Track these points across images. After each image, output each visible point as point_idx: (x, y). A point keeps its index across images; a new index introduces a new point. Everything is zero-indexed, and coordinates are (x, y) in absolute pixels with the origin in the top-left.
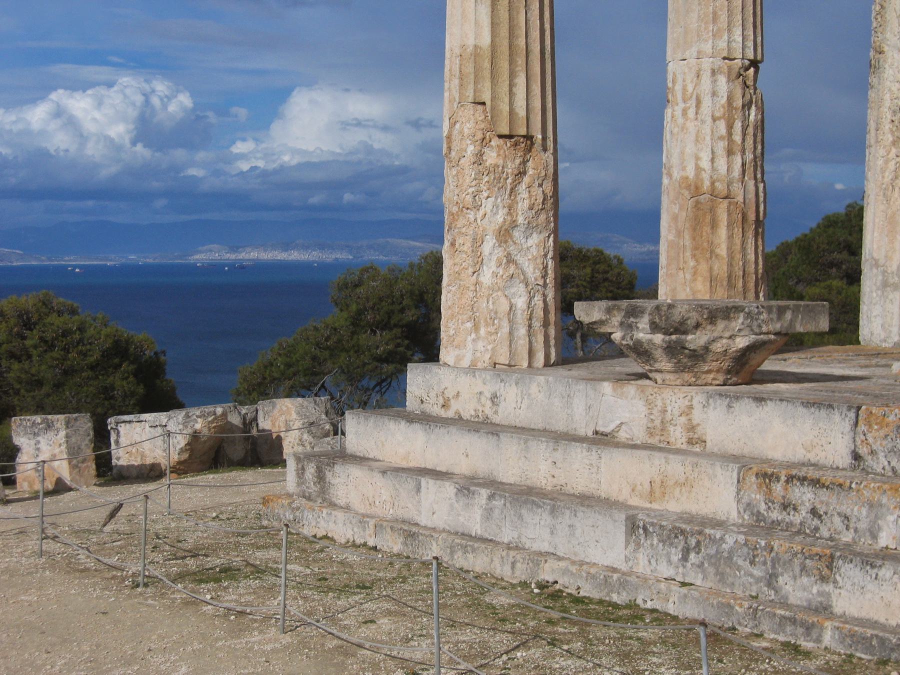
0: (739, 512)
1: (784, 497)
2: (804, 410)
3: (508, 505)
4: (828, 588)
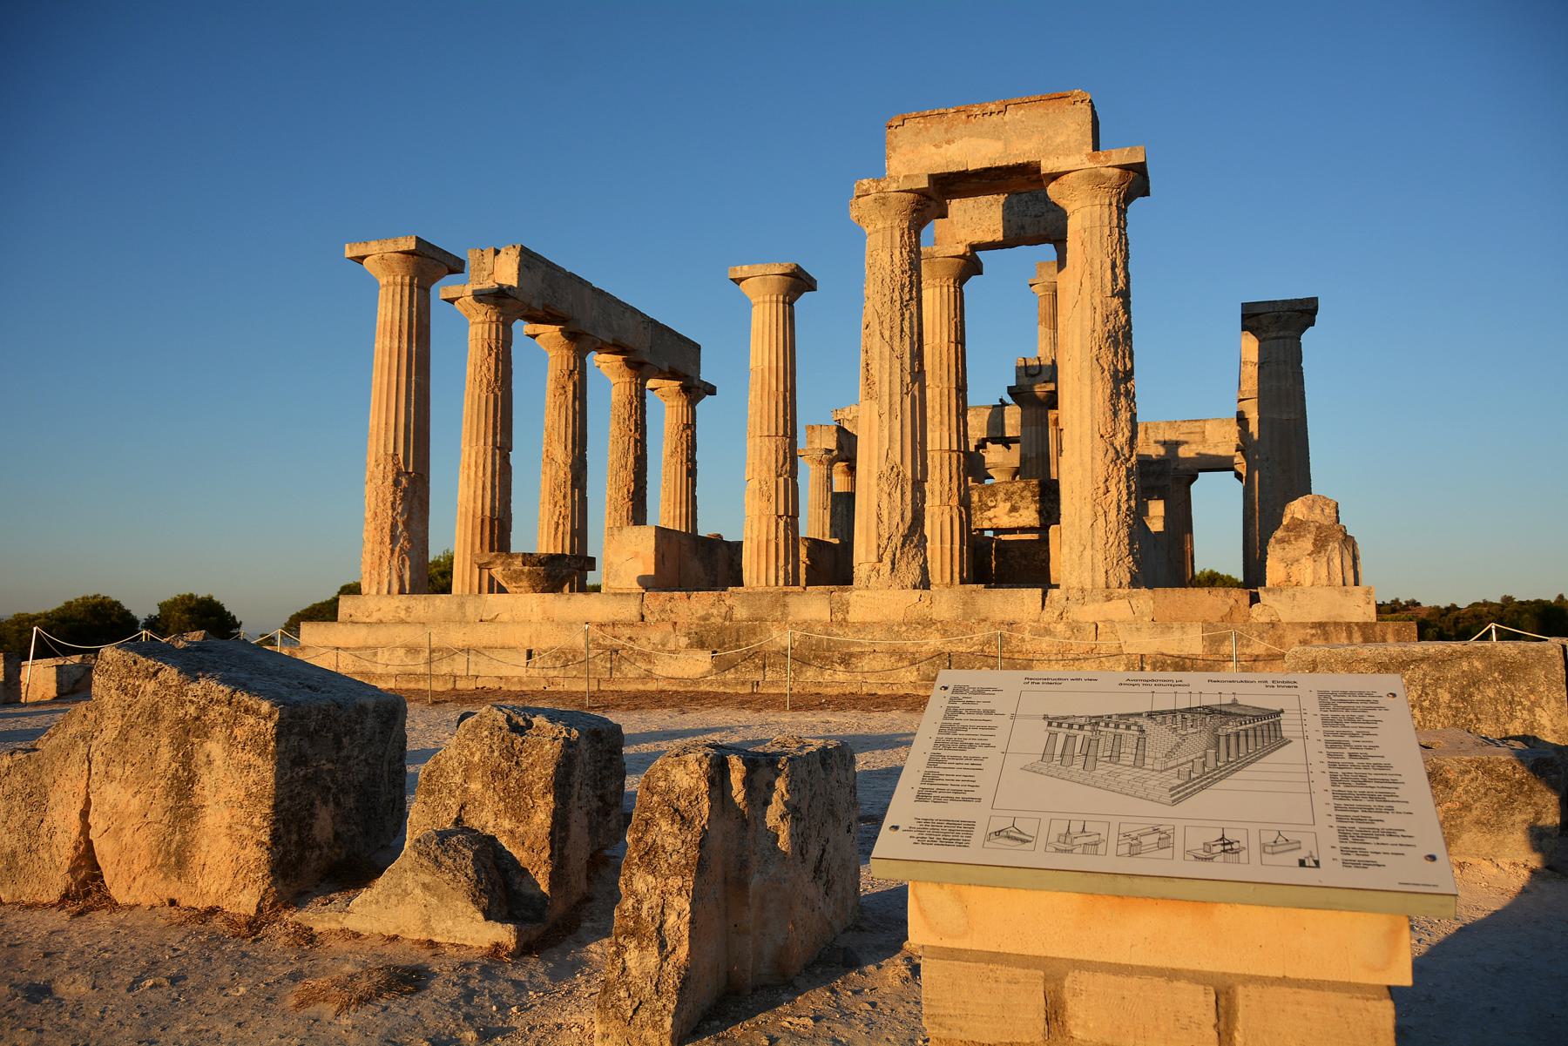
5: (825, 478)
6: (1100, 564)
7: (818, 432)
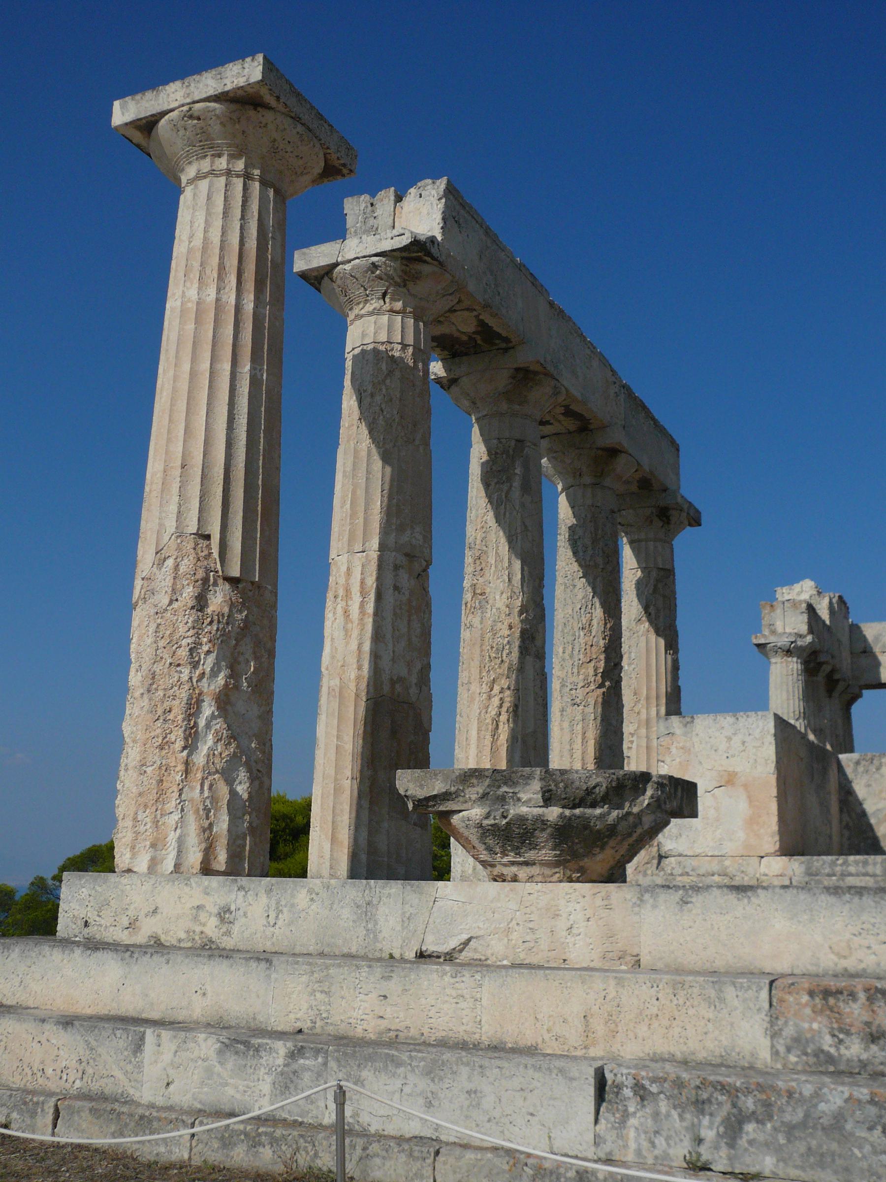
0: (775, 1053)
1: (868, 1024)
2: (832, 899)
3: (332, 1064)
5: (795, 675)
7: (779, 611)
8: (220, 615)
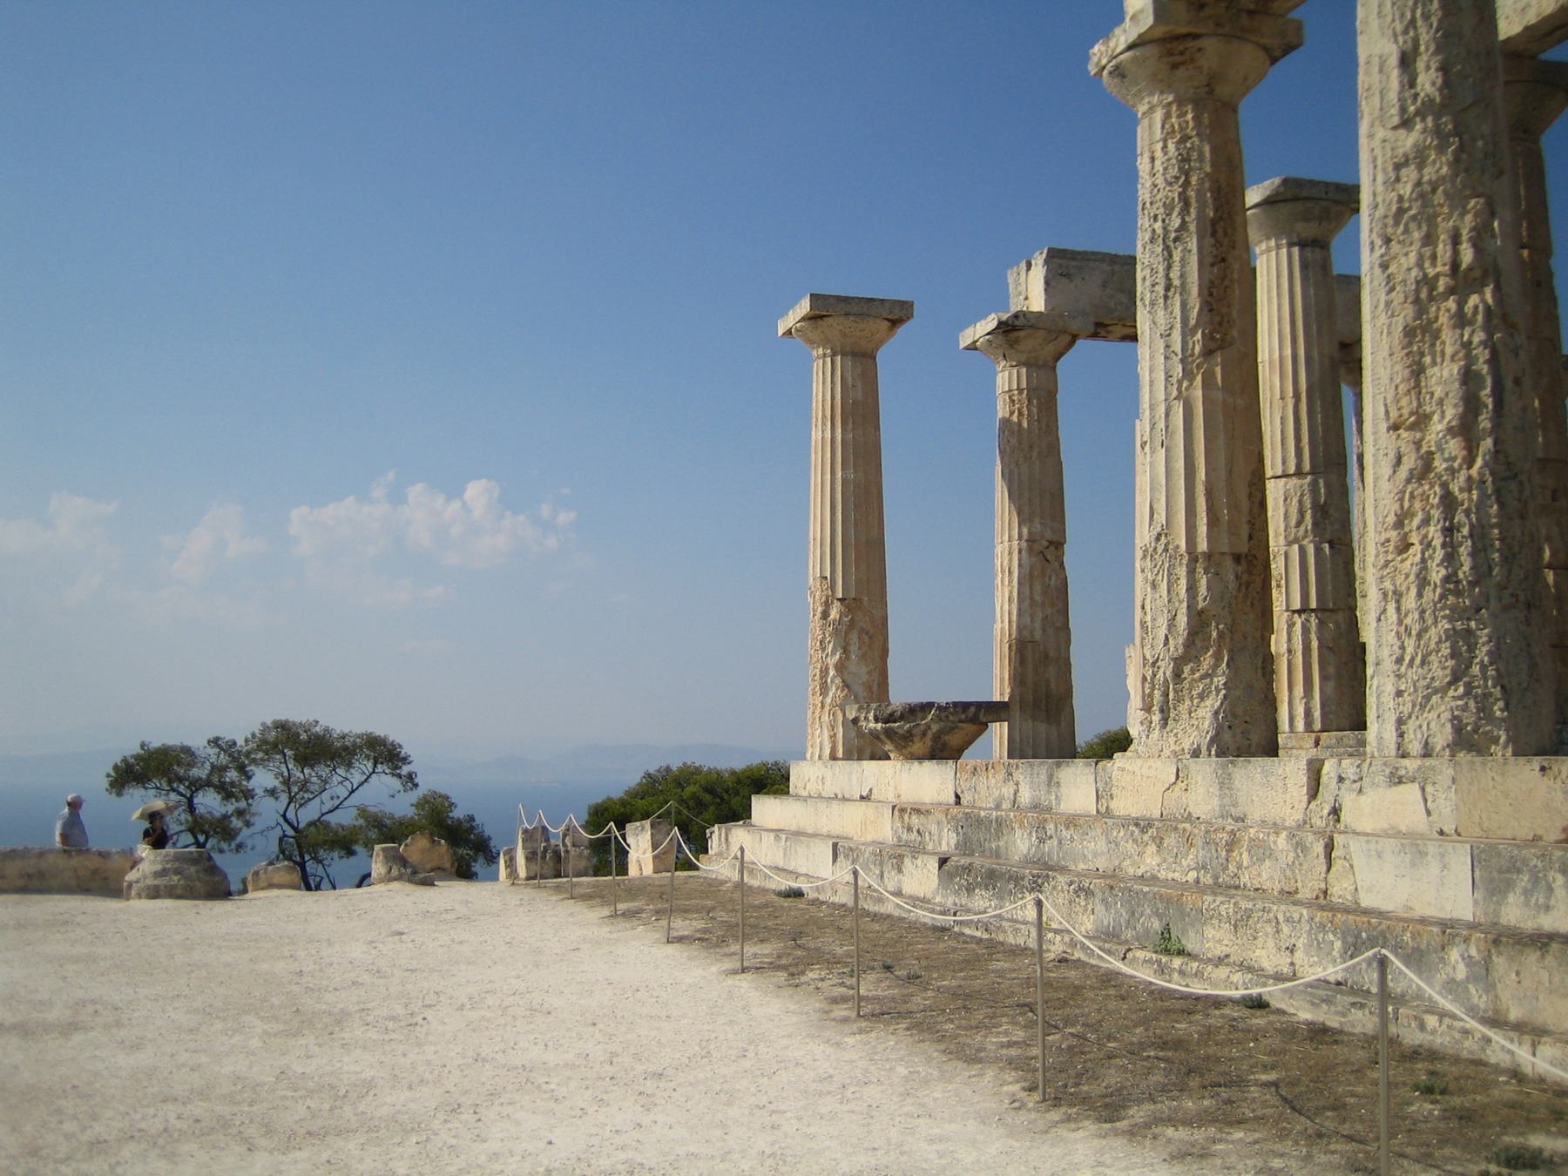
4: (901, 876)
6: (1391, 705)
8: (835, 620)
